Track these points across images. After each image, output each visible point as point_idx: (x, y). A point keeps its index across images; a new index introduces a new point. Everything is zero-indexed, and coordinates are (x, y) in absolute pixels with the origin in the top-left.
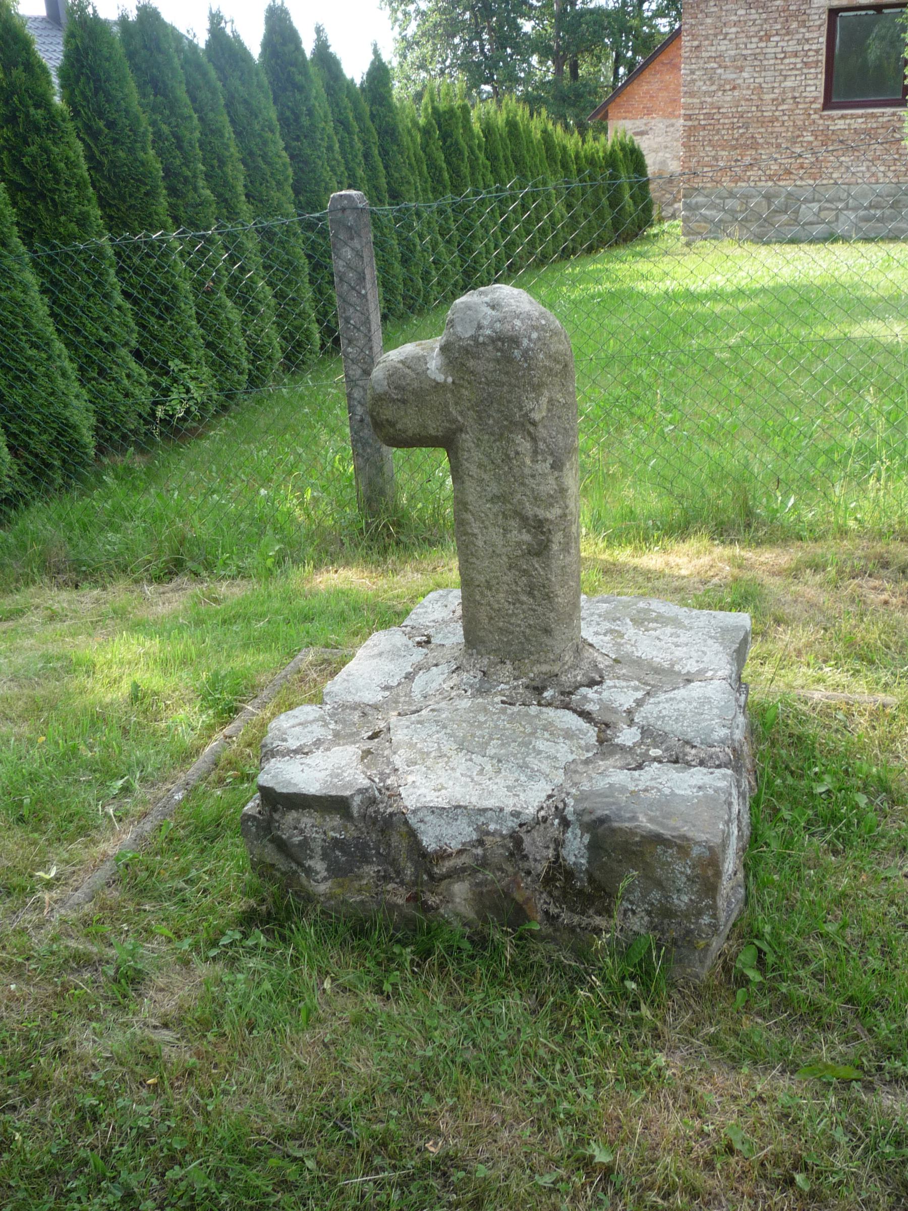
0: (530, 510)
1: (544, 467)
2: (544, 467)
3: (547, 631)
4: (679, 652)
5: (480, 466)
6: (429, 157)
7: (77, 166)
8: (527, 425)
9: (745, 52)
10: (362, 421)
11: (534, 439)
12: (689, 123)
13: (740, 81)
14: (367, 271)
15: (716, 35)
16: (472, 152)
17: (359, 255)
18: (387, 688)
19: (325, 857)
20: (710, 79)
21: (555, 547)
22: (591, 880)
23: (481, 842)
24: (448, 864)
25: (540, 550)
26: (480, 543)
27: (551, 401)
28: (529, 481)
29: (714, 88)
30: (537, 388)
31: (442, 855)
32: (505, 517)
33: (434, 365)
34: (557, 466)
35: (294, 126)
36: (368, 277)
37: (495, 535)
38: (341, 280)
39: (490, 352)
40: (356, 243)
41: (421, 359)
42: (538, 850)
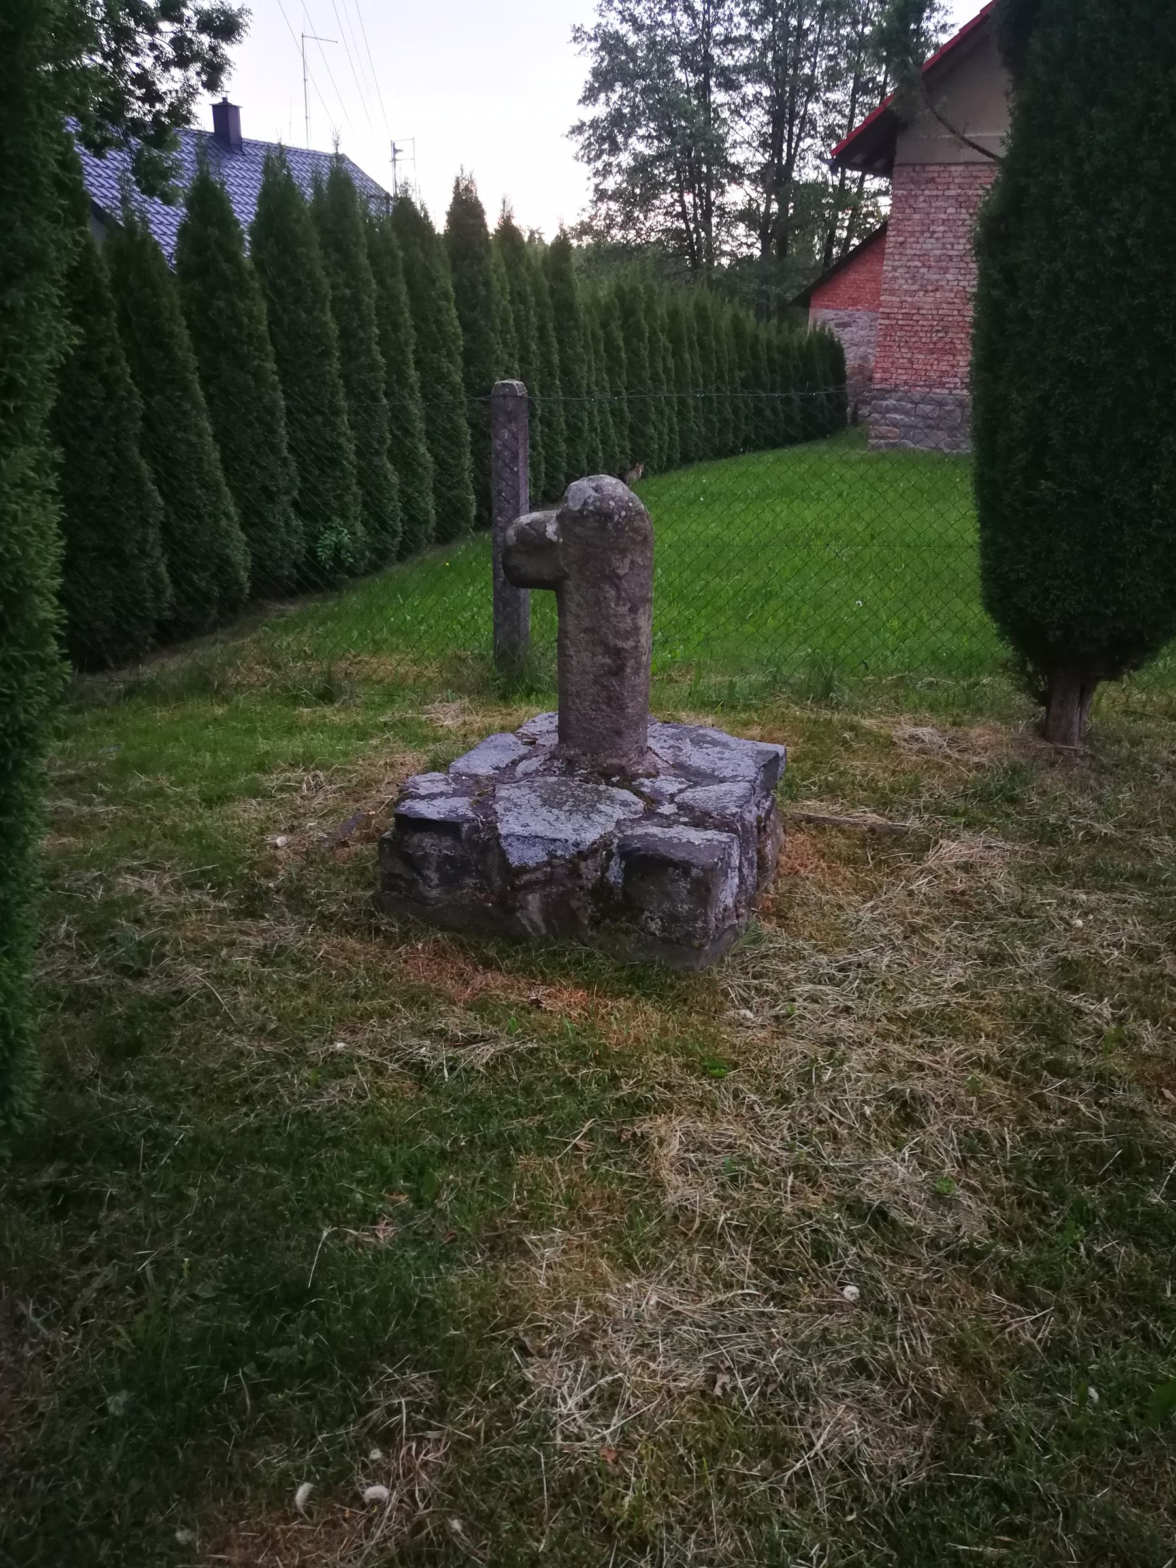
0: (612, 640)
1: (623, 609)
2: (623, 609)
3: (619, 733)
4: (720, 764)
5: (579, 605)
6: (608, 335)
7: (259, 323)
8: (614, 579)
9: (951, 253)
11: (618, 589)
12: (887, 322)
13: (944, 283)
14: (521, 451)
15: (922, 232)
16: (653, 333)
17: (515, 437)
18: (497, 768)
19: (438, 869)
20: (913, 278)
21: (628, 670)
22: (625, 894)
23: (549, 863)
24: (526, 877)
25: (617, 671)
26: (574, 663)
27: (632, 562)
28: (613, 619)
29: (916, 287)
30: (623, 552)
31: (523, 870)
32: (594, 644)
33: (551, 529)
34: (633, 610)
35: (470, 295)
36: (521, 456)
37: (585, 657)
38: (497, 457)
39: (592, 523)
40: (513, 427)
41: (543, 524)
42: (589, 869)
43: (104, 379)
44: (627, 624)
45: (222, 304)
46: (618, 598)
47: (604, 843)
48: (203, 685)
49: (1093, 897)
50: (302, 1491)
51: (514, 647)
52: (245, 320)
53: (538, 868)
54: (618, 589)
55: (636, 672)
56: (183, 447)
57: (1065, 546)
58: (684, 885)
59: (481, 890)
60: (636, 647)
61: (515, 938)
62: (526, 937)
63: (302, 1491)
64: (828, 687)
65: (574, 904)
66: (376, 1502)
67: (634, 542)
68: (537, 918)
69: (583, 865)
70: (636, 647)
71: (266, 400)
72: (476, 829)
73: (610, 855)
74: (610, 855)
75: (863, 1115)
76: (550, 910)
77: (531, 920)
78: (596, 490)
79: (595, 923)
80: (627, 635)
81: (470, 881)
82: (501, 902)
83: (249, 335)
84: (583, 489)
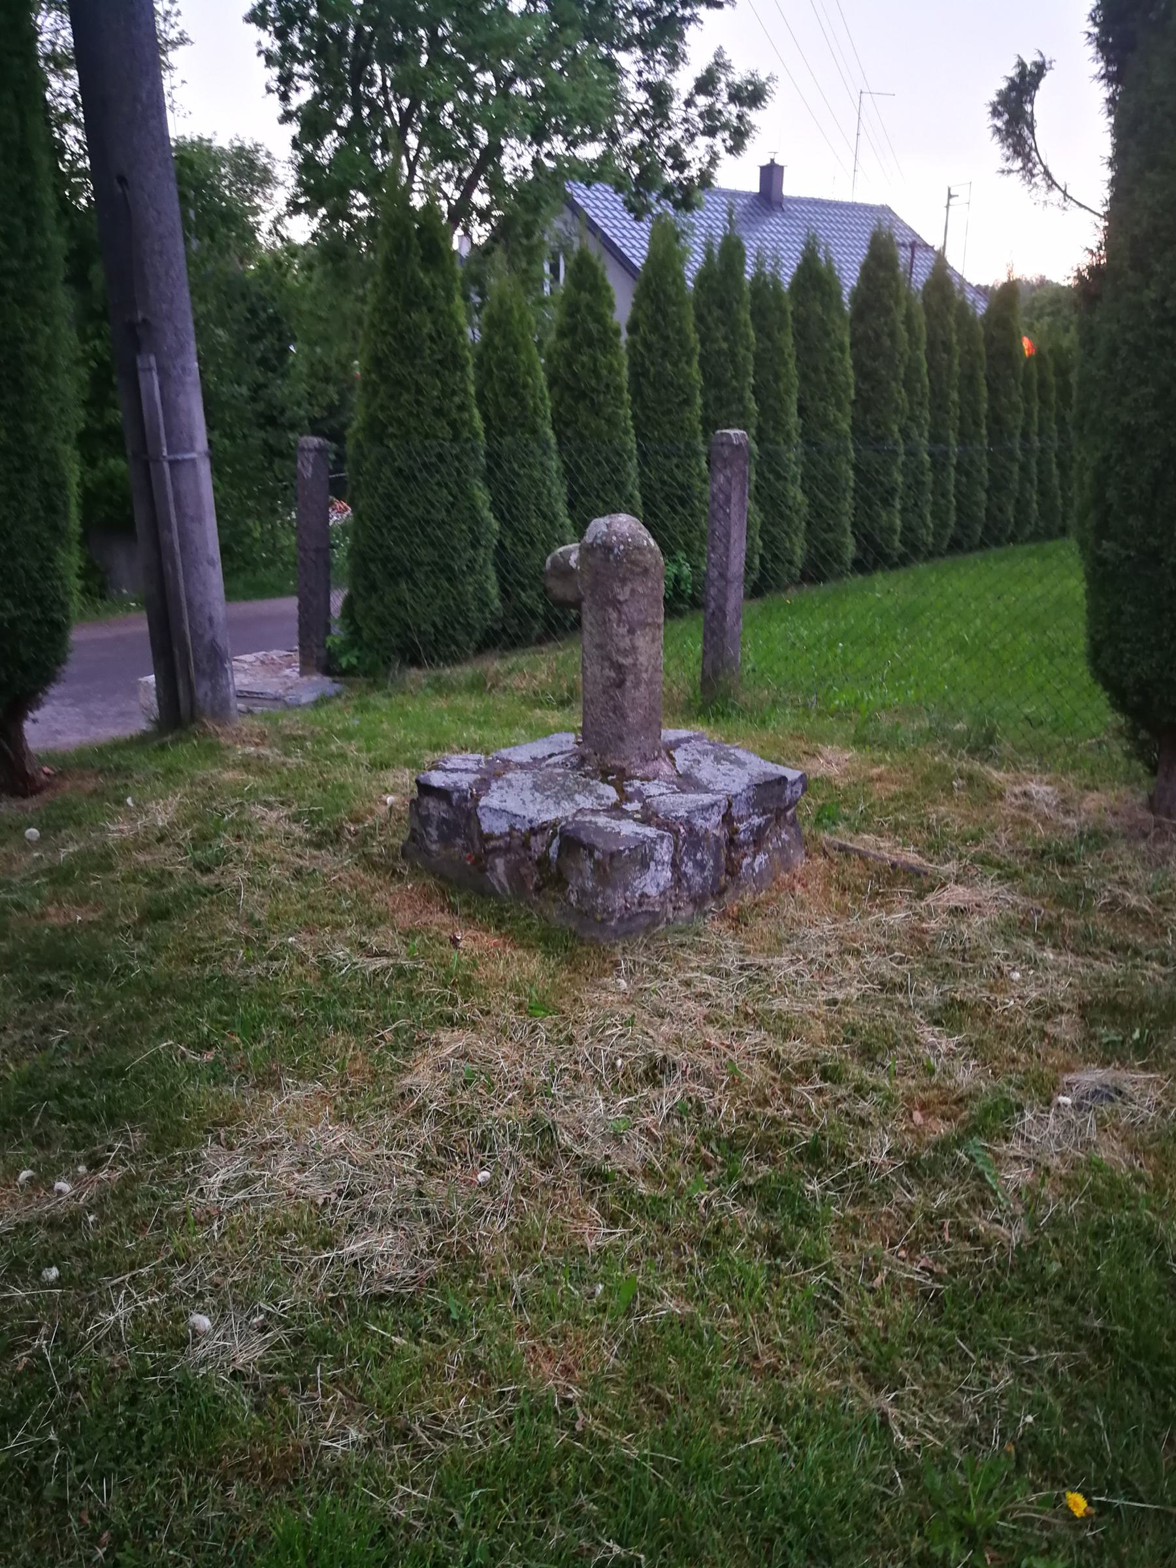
2: (623, 630)
3: (621, 739)
7: (619, 374)
10: (713, 614)
11: (620, 612)
17: (728, 481)
19: (438, 828)
21: (628, 684)
22: (558, 868)
23: (509, 834)
24: (493, 843)
25: (620, 684)
30: (623, 581)
31: (490, 837)
34: (631, 631)
35: (869, 346)
37: (596, 669)
40: (728, 473)
42: (537, 843)
43: (452, 424)
44: (626, 643)
45: (585, 359)
46: (620, 620)
47: (554, 824)
48: (478, 686)
49: (1061, 958)
50: (25, 1174)
51: (716, 673)
52: (604, 372)
53: (501, 836)
54: (620, 612)
55: (636, 686)
56: (526, 481)
57: (1131, 609)
58: (588, 865)
59: (467, 850)
60: (635, 665)
61: (484, 892)
62: (494, 893)
63: (25, 1174)
64: (990, 739)
65: (523, 871)
66: (60, 1193)
67: (632, 572)
68: (504, 880)
69: (533, 839)
70: (635, 665)
71: (616, 442)
72: (465, 799)
73: (554, 836)
74: (554, 836)
75: (614, 1065)
76: (513, 872)
77: (499, 882)
78: (608, 526)
79: (538, 889)
80: (625, 653)
81: (459, 842)
82: (478, 860)
83: (607, 386)
84: (599, 526)
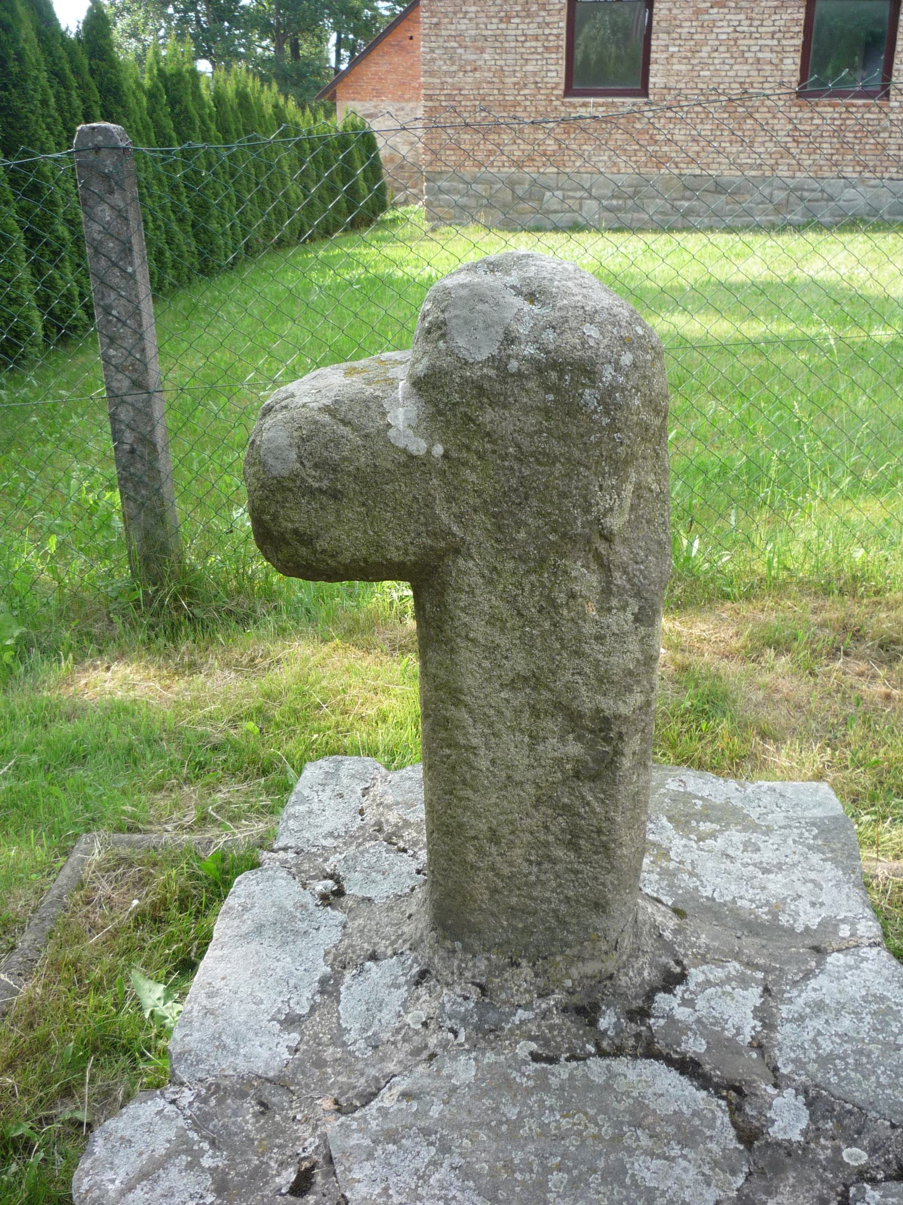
0: (588, 700)
1: (621, 620)
2: (621, 620)
4: (776, 884)
5: (493, 620)
6: (157, 124)
8: (596, 541)
9: (485, 33)
10: (132, 451)
11: (605, 567)
12: (430, 104)
13: (481, 63)
14: (135, 240)
15: (455, 13)
16: (203, 122)
18: (291, 1022)
20: (451, 58)
21: (627, 762)
26: (483, 764)
27: (638, 487)
28: (593, 649)
29: (455, 68)
32: (536, 713)
33: (402, 417)
36: (136, 248)
37: (514, 749)
38: (97, 252)
39: (534, 393)
40: (117, 199)
41: (373, 405)
54: (605, 567)
